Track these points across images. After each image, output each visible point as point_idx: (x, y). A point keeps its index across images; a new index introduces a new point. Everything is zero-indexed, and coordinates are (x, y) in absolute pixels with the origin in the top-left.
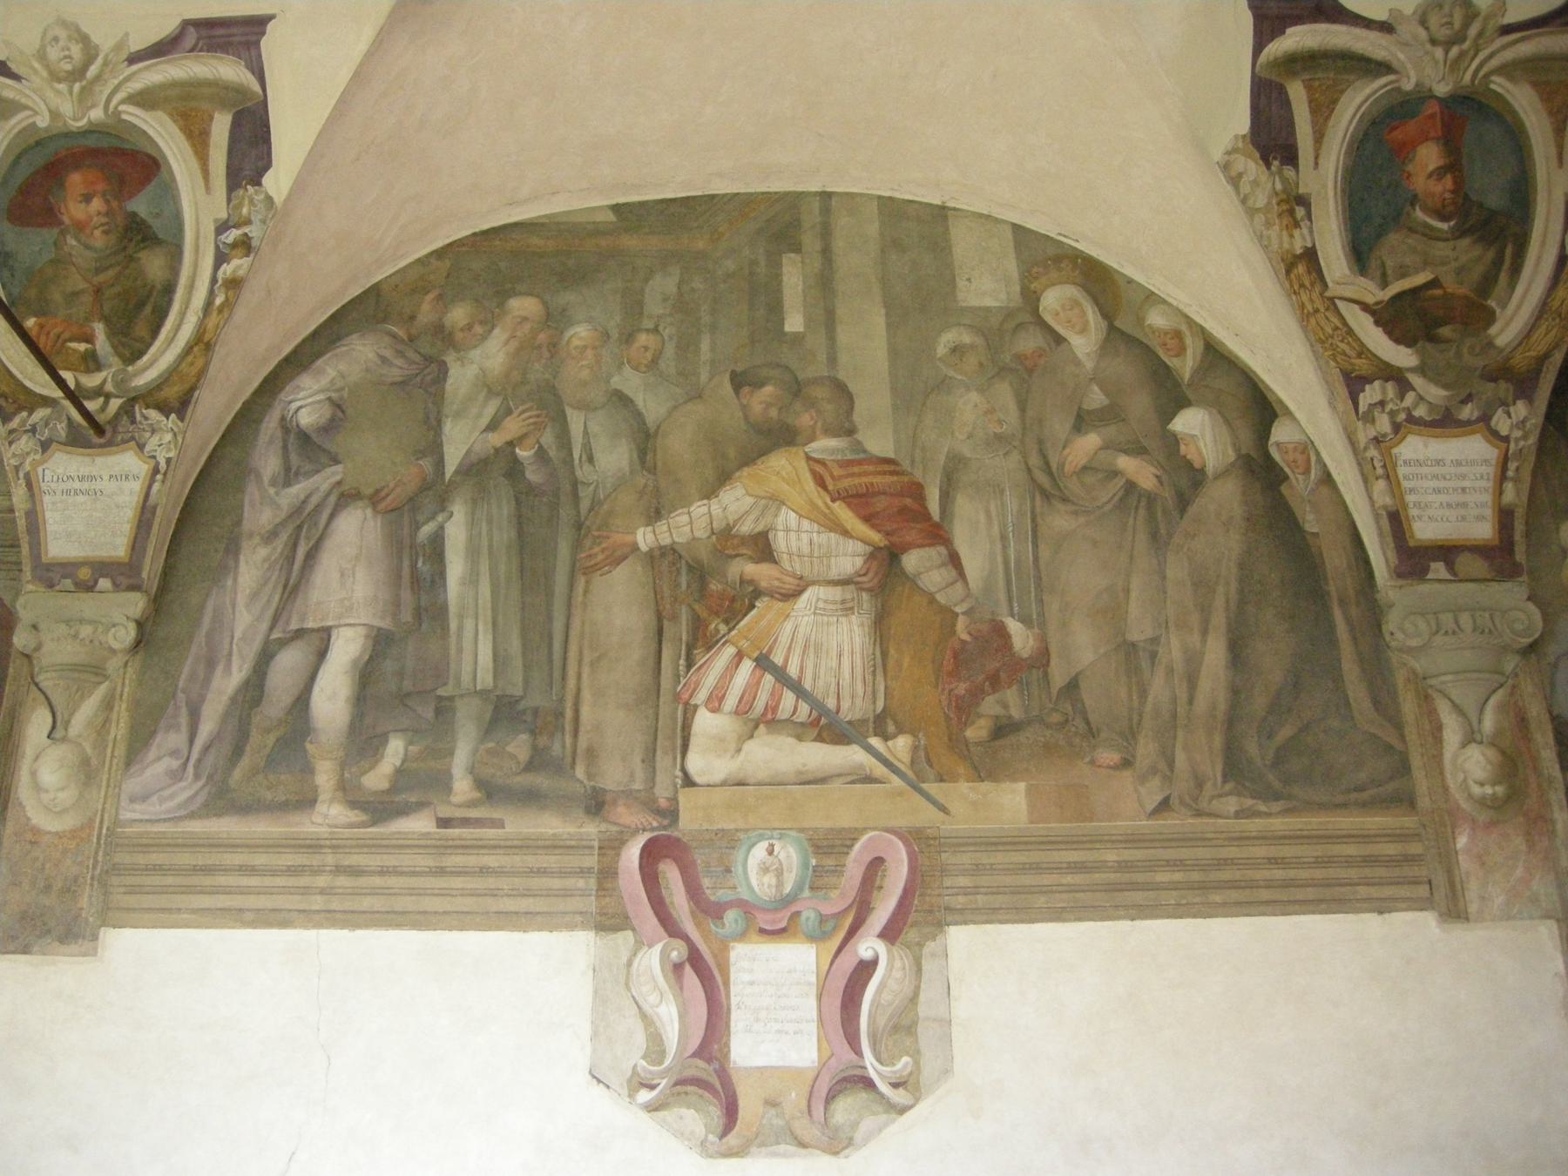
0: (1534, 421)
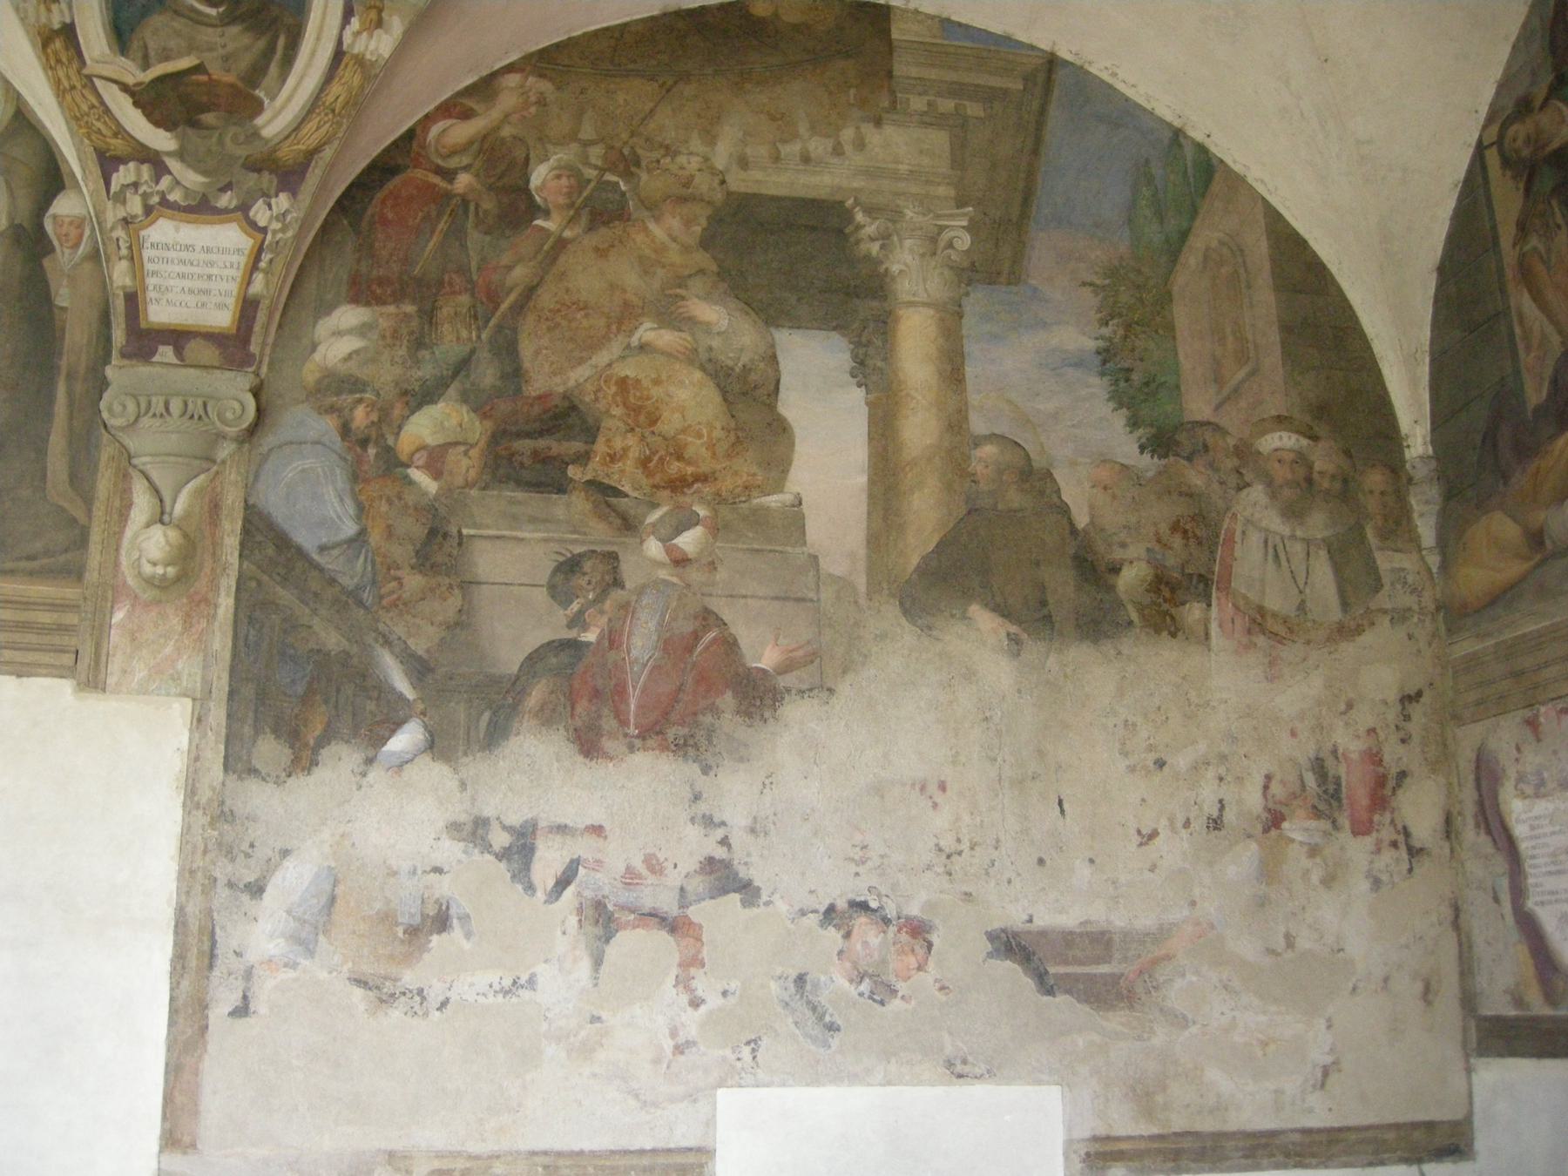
0: (295, 215)
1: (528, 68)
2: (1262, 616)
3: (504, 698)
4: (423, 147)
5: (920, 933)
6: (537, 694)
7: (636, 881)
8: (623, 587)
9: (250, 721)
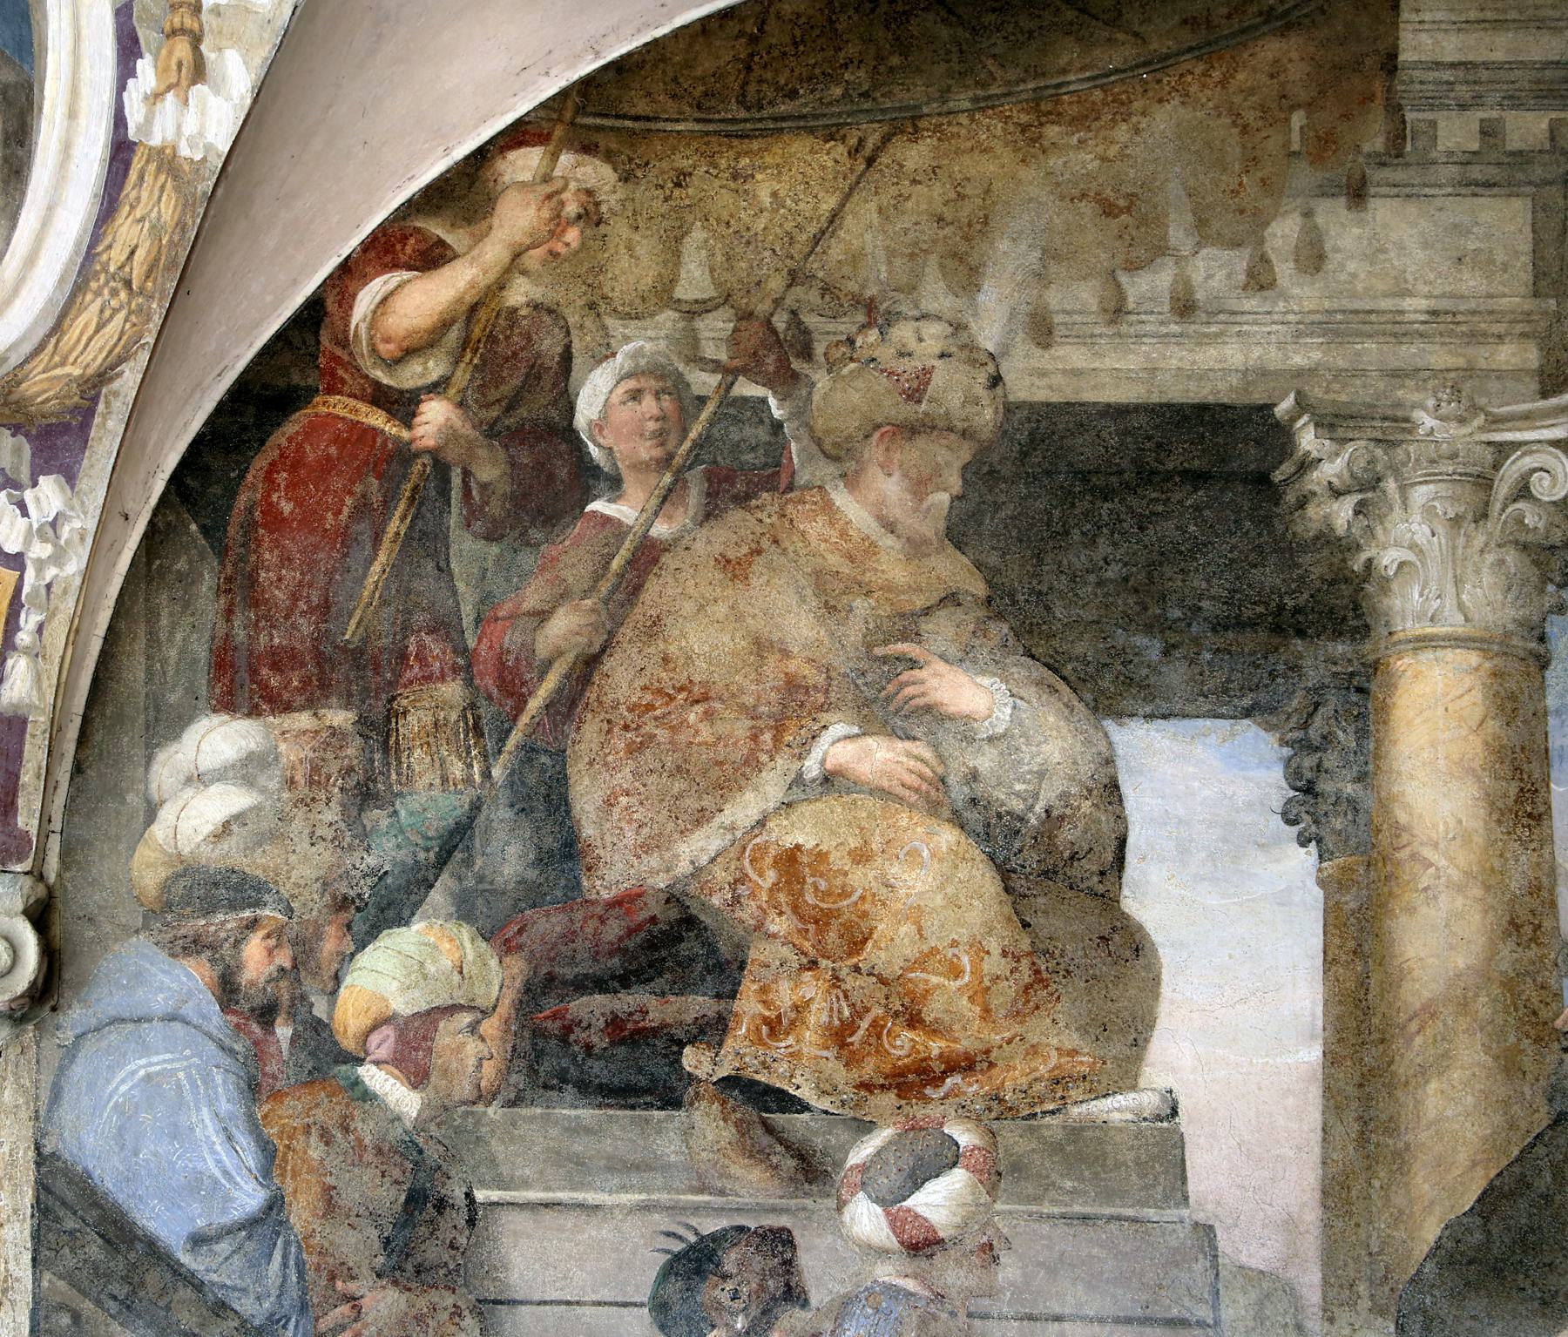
1: (558, 132)
8: (805, 1304)
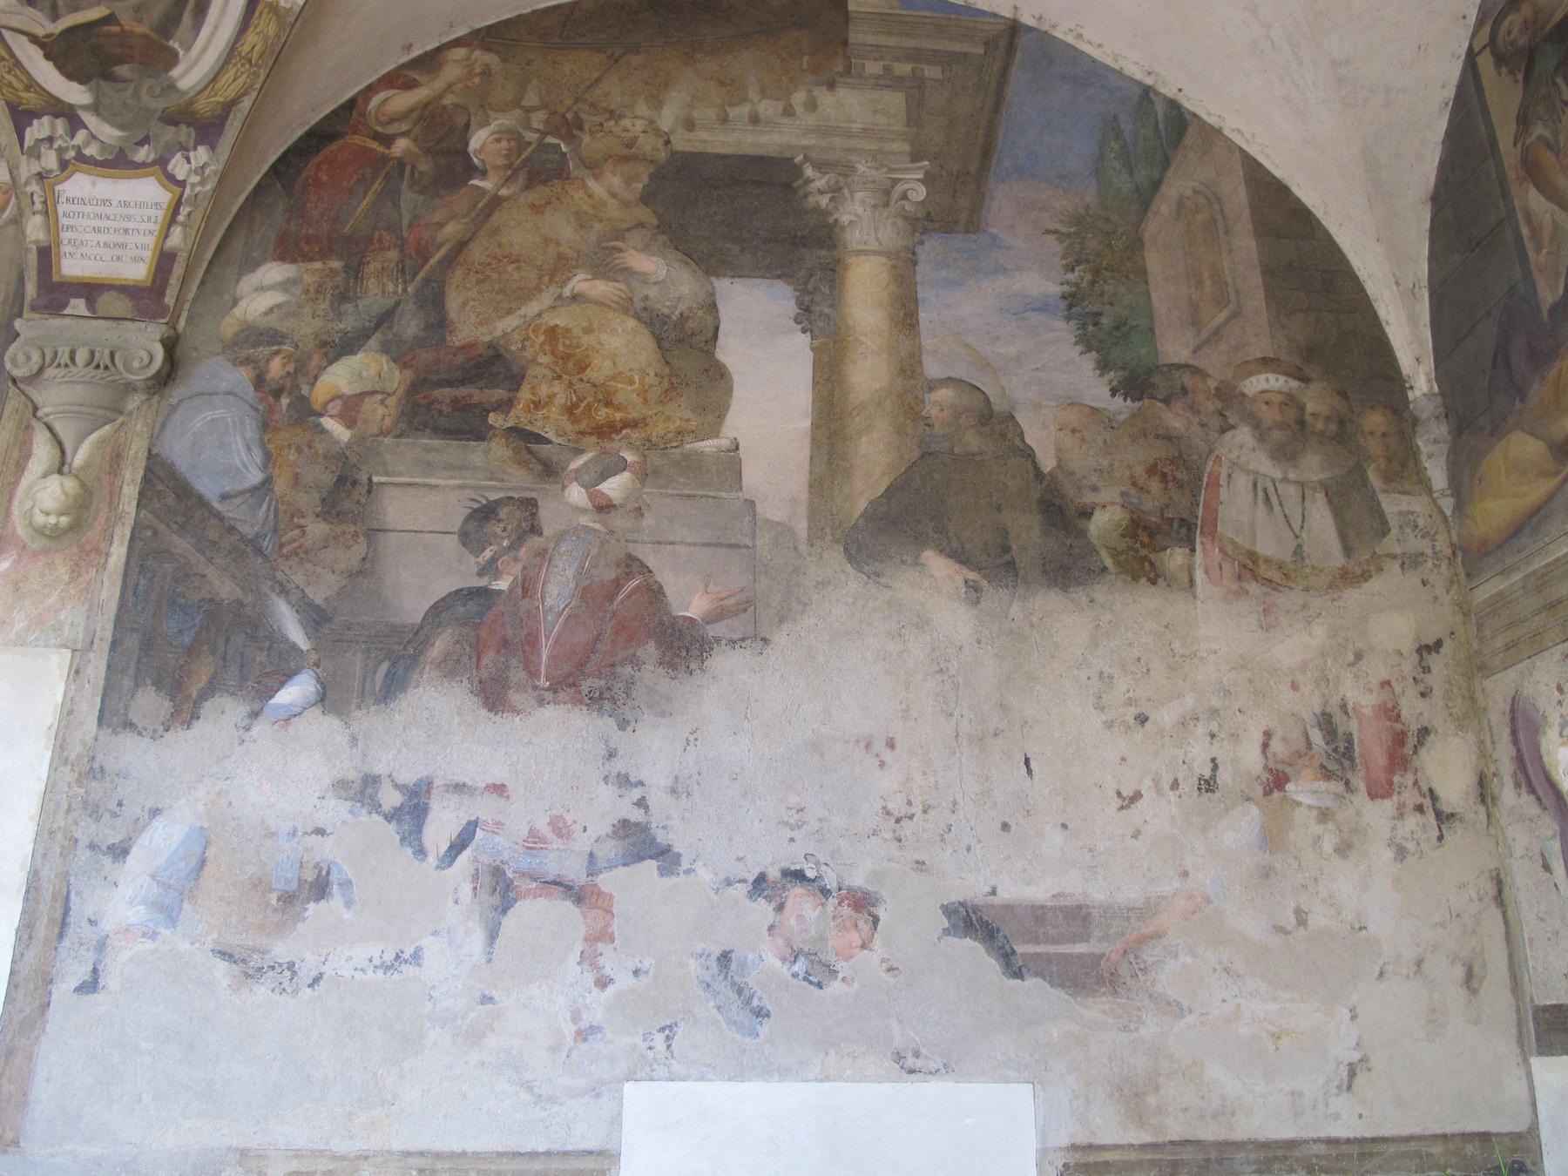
0: (213, 168)
2: (1253, 562)
3: (405, 648)
4: (363, 115)
5: (863, 907)
6: (440, 645)
7: (539, 845)
8: (541, 534)
9: (131, 672)
